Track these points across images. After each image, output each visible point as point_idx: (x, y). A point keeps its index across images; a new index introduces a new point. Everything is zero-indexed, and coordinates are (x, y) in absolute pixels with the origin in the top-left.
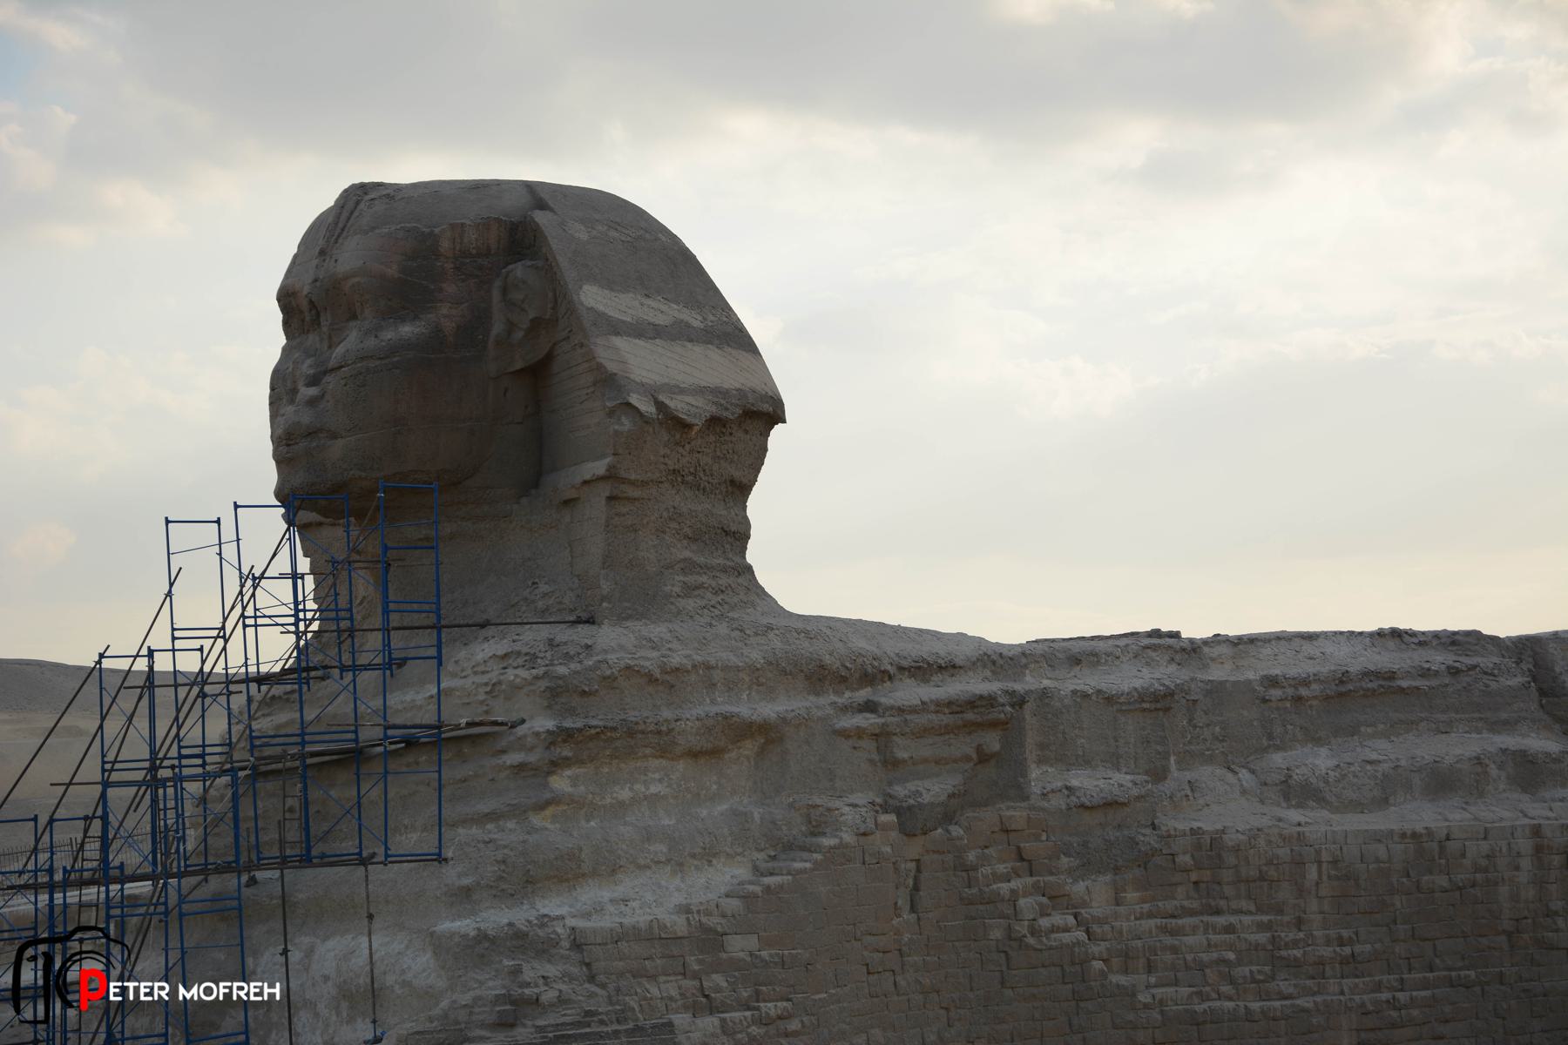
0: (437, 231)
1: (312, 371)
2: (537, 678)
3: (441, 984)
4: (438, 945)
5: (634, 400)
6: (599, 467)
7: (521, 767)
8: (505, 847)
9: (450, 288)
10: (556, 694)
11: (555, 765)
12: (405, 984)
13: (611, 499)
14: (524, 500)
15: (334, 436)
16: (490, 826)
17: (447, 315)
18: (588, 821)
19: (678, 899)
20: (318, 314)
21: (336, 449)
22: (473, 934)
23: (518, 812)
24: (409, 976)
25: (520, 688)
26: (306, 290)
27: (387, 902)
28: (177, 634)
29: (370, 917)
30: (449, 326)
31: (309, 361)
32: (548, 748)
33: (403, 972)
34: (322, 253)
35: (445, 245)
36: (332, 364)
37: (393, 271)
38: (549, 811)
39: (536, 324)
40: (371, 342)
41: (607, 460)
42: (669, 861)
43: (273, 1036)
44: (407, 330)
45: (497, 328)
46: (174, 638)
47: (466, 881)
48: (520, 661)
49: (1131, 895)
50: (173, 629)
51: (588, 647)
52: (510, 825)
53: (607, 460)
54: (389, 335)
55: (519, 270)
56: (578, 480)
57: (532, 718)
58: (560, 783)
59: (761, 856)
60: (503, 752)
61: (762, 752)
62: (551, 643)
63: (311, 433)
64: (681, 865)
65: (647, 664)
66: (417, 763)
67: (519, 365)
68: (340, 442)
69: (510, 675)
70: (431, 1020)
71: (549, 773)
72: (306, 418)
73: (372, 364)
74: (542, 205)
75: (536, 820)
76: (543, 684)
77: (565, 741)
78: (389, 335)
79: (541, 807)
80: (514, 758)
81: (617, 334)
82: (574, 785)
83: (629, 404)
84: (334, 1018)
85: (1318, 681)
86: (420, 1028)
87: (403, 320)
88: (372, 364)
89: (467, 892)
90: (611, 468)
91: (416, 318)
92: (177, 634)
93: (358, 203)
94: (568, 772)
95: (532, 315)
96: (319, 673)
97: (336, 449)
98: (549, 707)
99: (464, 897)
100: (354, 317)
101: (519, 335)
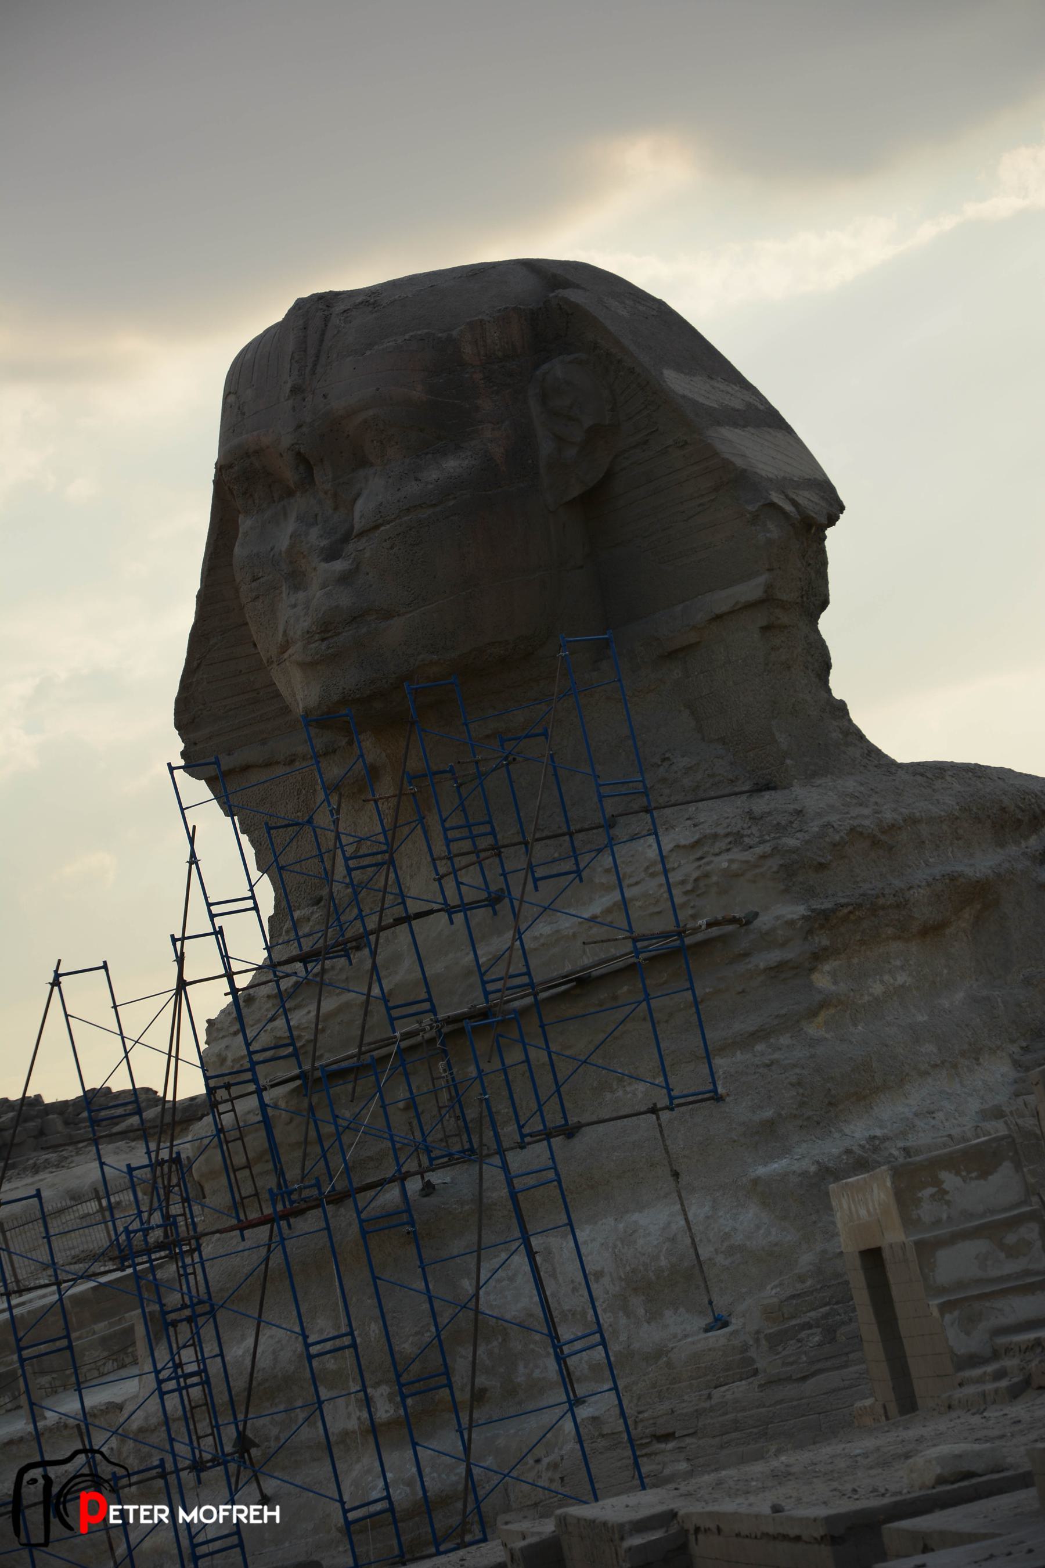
0: (455, 333)
1: (324, 543)
2: (764, 857)
4: (765, 1192)
5: (776, 498)
6: (751, 590)
7: (780, 967)
8: (795, 1066)
10: (794, 872)
11: (818, 957)
13: (766, 629)
16: (760, 1047)
18: (855, 1025)
19: (974, 1105)
20: (310, 469)
22: (813, 1169)
25: (737, 875)
26: (287, 441)
28: (215, 910)
29: (676, 1175)
31: (314, 532)
32: (805, 939)
34: (296, 390)
36: (358, 527)
38: (820, 1019)
42: (943, 1063)
43: (521, 1369)
44: (453, 465)
46: (212, 916)
47: (768, 1113)
48: (722, 844)
50: (209, 905)
51: (799, 813)
52: (785, 1040)
53: (762, 579)
54: (432, 475)
55: (557, 368)
58: (822, 980)
59: (1015, 1048)
60: (746, 955)
62: (753, 818)
64: (955, 1066)
65: (866, 823)
69: (722, 862)
70: (801, 1279)
71: (812, 970)
72: (345, 599)
74: (566, 284)
75: (813, 1029)
76: (774, 863)
77: (822, 927)
78: (432, 475)
79: (812, 1014)
81: (719, 424)
82: (835, 983)
83: (772, 505)
84: (623, 1321)
90: (769, 587)
92: (215, 910)
93: (326, 319)
94: (827, 967)
96: (354, 944)
98: (786, 891)
99: (767, 1134)
100: (362, 462)
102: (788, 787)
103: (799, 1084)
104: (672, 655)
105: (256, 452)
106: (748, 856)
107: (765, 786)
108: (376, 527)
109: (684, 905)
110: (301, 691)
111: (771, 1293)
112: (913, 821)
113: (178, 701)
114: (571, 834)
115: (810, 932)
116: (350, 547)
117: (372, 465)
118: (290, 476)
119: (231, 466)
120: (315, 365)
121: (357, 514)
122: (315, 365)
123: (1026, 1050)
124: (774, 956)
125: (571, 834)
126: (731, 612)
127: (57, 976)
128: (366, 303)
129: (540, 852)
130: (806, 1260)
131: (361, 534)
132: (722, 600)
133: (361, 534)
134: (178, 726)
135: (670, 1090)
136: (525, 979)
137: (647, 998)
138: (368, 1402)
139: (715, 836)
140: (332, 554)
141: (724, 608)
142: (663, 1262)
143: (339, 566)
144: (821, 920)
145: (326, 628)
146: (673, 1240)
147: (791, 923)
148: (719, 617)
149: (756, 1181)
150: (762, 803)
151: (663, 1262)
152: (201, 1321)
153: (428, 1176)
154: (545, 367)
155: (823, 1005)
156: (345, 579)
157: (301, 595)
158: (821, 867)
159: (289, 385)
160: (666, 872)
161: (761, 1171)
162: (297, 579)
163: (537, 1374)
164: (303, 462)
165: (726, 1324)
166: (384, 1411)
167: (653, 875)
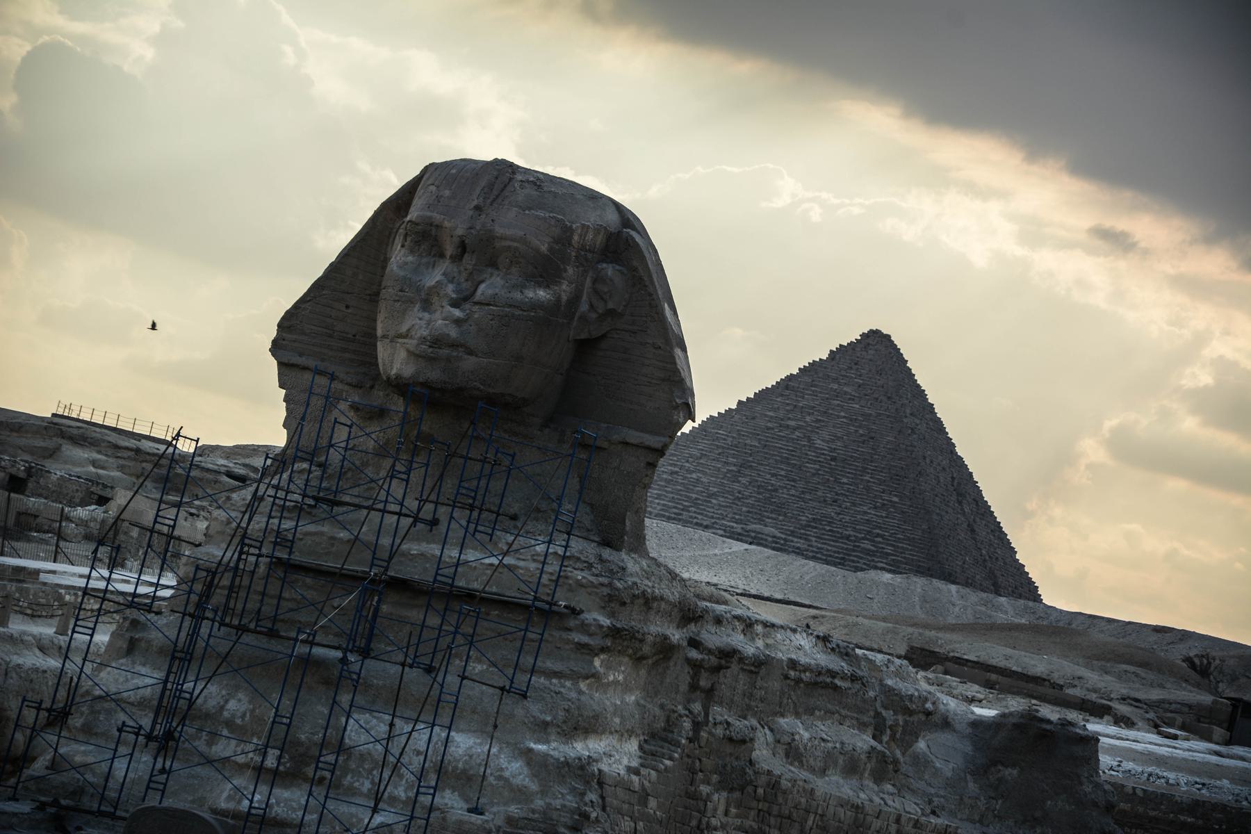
1: (454, 296)
2: (602, 585)
3: (534, 787)
9: (570, 270)
11: (603, 650)
12: (500, 778)
14: (547, 431)
15: (470, 352)
16: (554, 681)
17: (565, 289)
21: (469, 363)
23: (576, 677)
24: (507, 774)
25: (582, 586)
26: (460, 232)
27: (474, 712)
29: (495, 726)
30: (564, 298)
33: (502, 769)
35: (576, 238)
37: (544, 248)
39: (611, 313)
40: (517, 295)
41: (663, 439)
43: (349, 778)
44: (542, 294)
45: (584, 307)
47: (549, 719)
48: (578, 565)
49: (733, 811)
52: (568, 684)
54: (530, 294)
55: (610, 270)
56: (616, 437)
57: (589, 611)
58: (597, 662)
60: (570, 630)
61: (656, 664)
62: (601, 560)
63: (454, 345)
66: (488, 614)
67: (583, 337)
68: (473, 359)
69: (579, 576)
70: (534, 811)
71: (597, 655)
72: (453, 332)
73: (518, 312)
74: (634, 229)
75: (583, 686)
76: (606, 591)
80: (578, 637)
85: (811, 671)
86: (524, 815)
87: (539, 285)
88: (518, 312)
89: (545, 725)
91: (548, 287)
95: (610, 305)
97: (469, 363)
98: (604, 608)
99: (542, 729)
101: (594, 316)
102: (618, 549)
103: (567, 711)
104: (585, 446)
105: (437, 226)
106: (592, 578)
107: (606, 543)
108: (488, 305)
109: (545, 586)
110: (395, 360)
111: (514, 810)
112: (662, 598)
113: (287, 312)
114: (498, 514)
115: (607, 636)
116: (467, 306)
117: (498, 269)
118: (449, 250)
119: (417, 224)
120: (494, 200)
121: (479, 291)
122: (494, 200)
123: (645, 741)
124: (585, 639)
125: (498, 514)
126: (637, 446)
127: (178, 435)
128: (534, 183)
129: (485, 515)
130: (539, 803)
131: (476, 303)
132: (634, 436)
133: (476, 303)
134: (279, 325)
135: (512, 682)
136: (450, 581)
137: (526, 630)
138: (265, 755)
139: (579, 559)
140: (455, 304)
141: (632, 441)
142: (460, 765)
143: (457, 313)
144: (615, 632)
145: (437, 341)
146: (471, 757)
147: (601, 627)
148: (627, 444)
149: (531, 750)
150: (607, 553)
151: (460, 765)
152: (420, 726)
153: (349, 654)
154: (605, 265)
155: (593, 676)
156: (458, 322)
157: (426, 315)
158: (624, 604)
159: (475, 203)
160: (544, 563)
161: (532, 745)
162: (427, 305)
163: (357, 784)
164: (463, 248)
165: (482, 814)
166: (271, 762)
167: (534, 560)
